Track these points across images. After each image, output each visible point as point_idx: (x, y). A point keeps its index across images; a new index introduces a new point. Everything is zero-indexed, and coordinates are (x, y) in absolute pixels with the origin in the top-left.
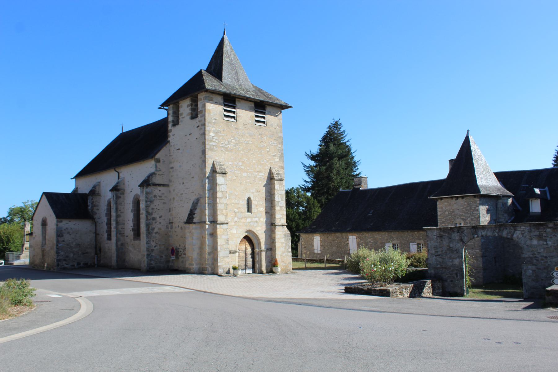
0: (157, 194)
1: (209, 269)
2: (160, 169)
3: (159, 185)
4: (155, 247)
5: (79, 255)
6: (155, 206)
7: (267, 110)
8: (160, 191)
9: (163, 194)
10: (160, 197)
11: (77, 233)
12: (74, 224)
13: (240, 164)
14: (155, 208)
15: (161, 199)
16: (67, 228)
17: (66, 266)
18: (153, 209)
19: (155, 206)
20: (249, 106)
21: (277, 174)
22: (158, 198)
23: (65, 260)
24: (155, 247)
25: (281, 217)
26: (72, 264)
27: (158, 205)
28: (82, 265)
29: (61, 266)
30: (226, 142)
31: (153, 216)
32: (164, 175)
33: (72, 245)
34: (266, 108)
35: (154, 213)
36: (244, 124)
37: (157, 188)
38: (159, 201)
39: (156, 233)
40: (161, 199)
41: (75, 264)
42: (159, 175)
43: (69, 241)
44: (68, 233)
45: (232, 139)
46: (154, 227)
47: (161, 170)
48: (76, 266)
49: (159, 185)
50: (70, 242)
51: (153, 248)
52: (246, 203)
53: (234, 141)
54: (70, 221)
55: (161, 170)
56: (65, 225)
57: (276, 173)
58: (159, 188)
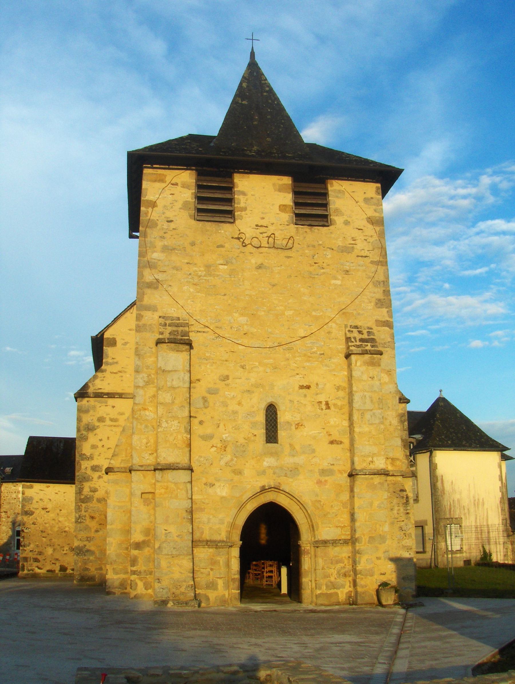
0: (105, 416)
1: (136, 584)
2: (115, 361)
3: (111, 395)
4: (97, 531)
5: (65, 552)
6: (101, 440)
7: (332, 188)
8: (113, 407)
9: (122, 414)
10: (112, 420)
11: (61, 510)
12: (57, 492)
13: (243, 320)
14: (100, 444)
15: (115, 426)
16: (41, 500)
17: (37, 571)
18: (94, 447)
19: (101, 440)
20: (274, 185)
21: (361, 340)
22: (108, 422)
23: (36, 560)
24: (97, 531)
25: (376, 452)
26: (48, 568)
27: (108, 438)
28: (69, 571)
29: (29, 570)
30: (200, 271)
31: (94, 462)
32: (125, 372)
33: (50, 532)
34: (329, 185)
35: (95, 457)
36: (257, 226)
37: (106, 402)
38: (112, 430)
39: (99, 500)
40: (115, 426)
41: (57, 568)
42: (111, 373)
43: (45, 523)
44: (43, 509)
45: (218, 262)
46: (97, 486)
47: (117, 363)
48: (57, 572)
49: (111, 395)
50: (47, 525)
51: (93, 534)
52: (261, 418)
53: (226, 267)
54: (48, 487)
55: (117, 363)
56: (37, 493)
57: (358, 339)
58: (111, 402)
